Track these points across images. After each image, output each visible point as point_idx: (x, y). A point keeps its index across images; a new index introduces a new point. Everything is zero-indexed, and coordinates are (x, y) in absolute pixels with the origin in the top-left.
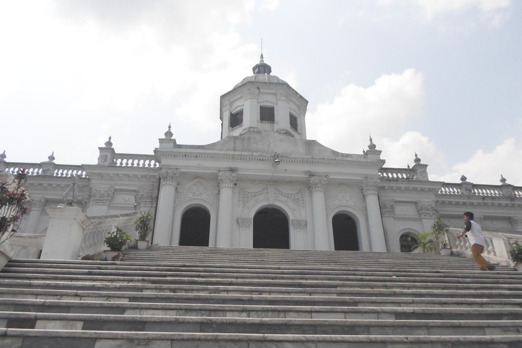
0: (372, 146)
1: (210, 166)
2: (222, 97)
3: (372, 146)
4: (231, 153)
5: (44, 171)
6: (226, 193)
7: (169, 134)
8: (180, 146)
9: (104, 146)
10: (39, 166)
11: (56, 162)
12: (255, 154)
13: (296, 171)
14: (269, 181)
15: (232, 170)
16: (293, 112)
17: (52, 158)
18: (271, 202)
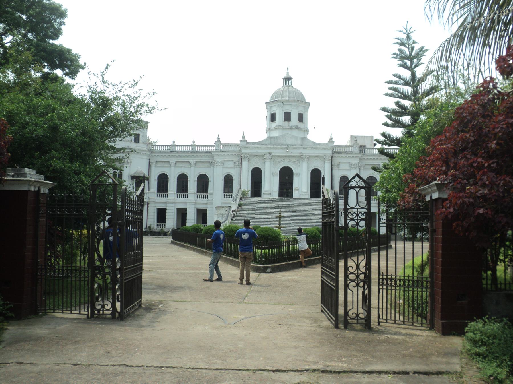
0: (331, 139)
1: (261, 152)
2: (266, 103)
3: (331, 139)
4: (269, 146)
5: (192, 149)
6: (268, 164)
7: (243, 137)
8: (248, 143)
9: (216, 140)
10: (190, 146)
11: (196, 144)
12: (279, 146)
13: (297, 152)
14: (285, 156)
15: (270, 154)
16: (301, 112)
17: (194, 142)
18: (286, 165)
